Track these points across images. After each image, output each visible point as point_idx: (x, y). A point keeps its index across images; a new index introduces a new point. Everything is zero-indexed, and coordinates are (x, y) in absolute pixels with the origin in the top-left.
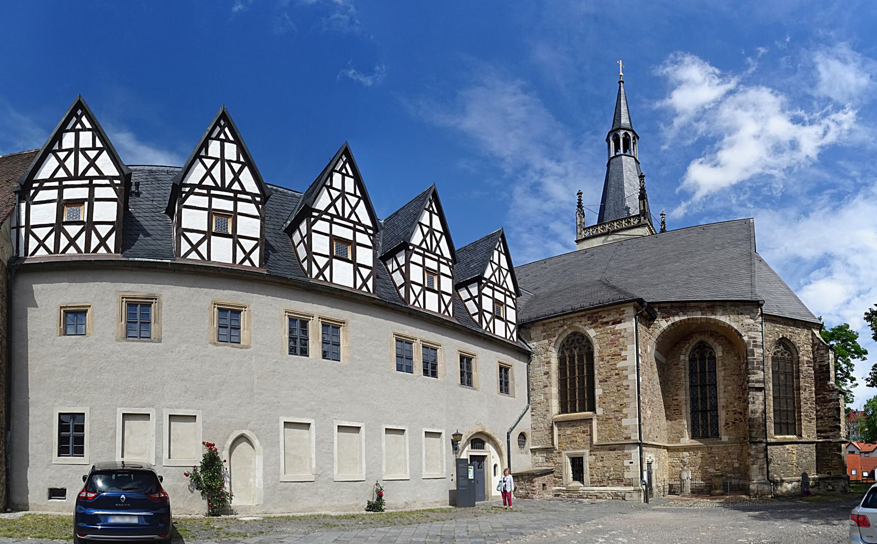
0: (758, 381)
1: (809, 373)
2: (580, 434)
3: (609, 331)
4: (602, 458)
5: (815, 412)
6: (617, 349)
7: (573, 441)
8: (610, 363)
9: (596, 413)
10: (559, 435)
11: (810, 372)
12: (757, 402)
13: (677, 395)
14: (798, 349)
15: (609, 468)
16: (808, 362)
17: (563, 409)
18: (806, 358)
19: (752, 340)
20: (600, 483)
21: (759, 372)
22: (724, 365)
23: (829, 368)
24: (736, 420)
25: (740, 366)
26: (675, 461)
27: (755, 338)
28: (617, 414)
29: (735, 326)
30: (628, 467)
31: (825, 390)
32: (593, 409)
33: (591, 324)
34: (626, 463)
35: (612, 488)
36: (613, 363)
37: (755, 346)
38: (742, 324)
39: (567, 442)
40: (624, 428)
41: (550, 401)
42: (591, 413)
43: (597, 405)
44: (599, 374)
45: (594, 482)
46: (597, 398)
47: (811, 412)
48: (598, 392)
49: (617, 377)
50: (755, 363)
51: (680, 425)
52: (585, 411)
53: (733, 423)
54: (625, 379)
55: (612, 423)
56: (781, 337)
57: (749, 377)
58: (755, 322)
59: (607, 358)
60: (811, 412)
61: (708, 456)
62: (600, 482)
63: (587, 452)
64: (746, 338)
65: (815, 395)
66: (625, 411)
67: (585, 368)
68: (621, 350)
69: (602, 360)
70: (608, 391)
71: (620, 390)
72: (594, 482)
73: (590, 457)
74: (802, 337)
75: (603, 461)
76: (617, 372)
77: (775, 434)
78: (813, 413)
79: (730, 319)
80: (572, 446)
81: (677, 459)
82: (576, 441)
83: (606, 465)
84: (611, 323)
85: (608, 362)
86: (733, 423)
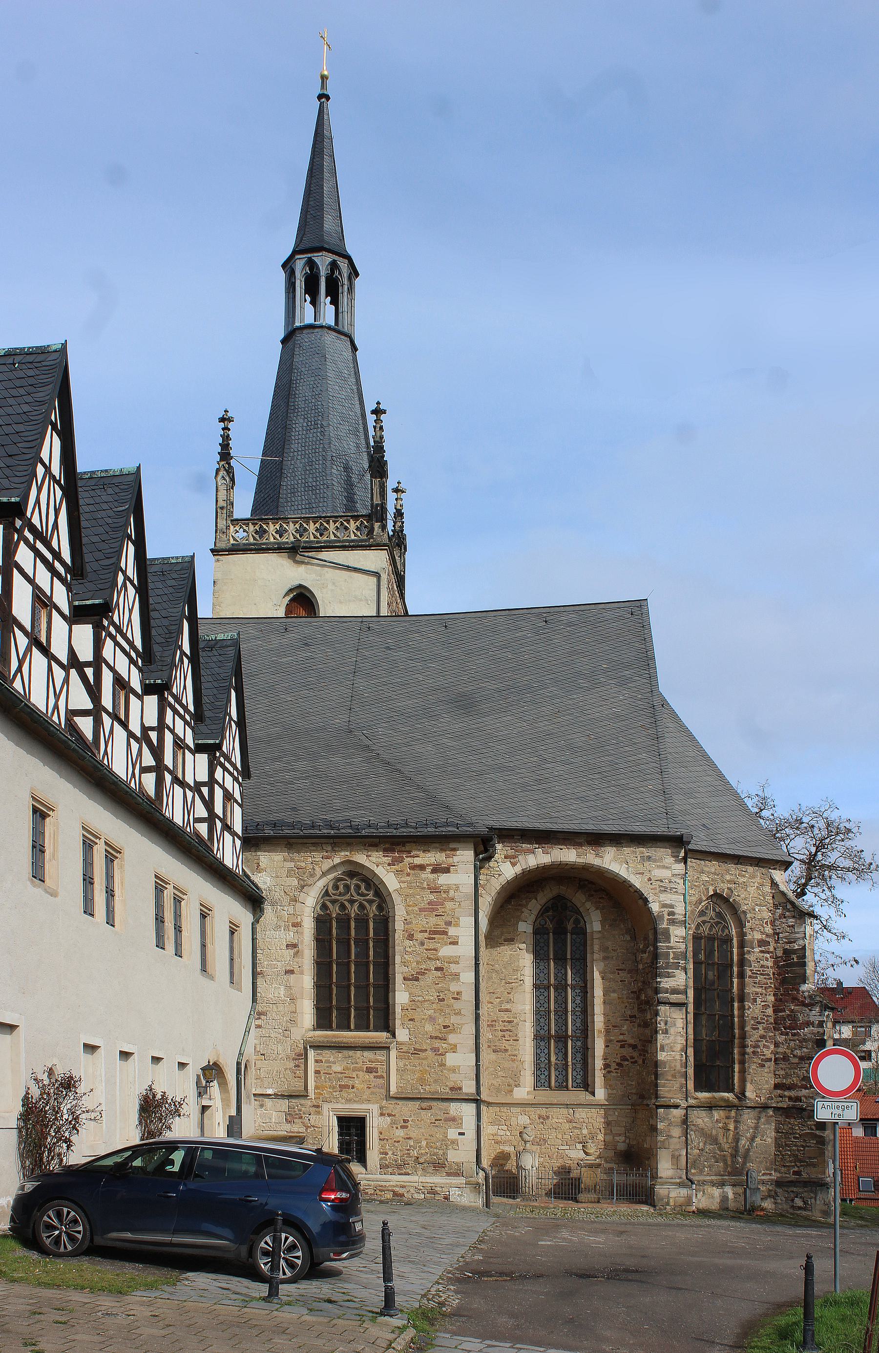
0: (675, 991)
1: (762, 966)
2: (361, 1073)
3: (425, 885)
4: (405, 1121)
5: (772, 1047)
6: (441, 922)
7: (346, 1087)
8: (425, 947)
9: (394, 1036)
10: (317, 1072)
11: (765, 963)
12: (672, 1031)
13: (509, 1001)
14: (742, 916)
15: (418, 1141)
16: (762, 943)
17: (323, 1020)
18: (758, 936)
19: (667, 910)
20: (400, 1168)
21: (677, 972)
22: (604, 949)
23: (804, 956)
24: (624, 1059)
25: (635, 954)
26: (501, 1133)
27: (672, 906)
28: (437, 1044)
29: (637, 882)
30: (454, 1142)
31: (794, 999)
32: (386, 1024)
33: (389, 865)
34: (452, 1134)
35: (422, 1179)
36: (431, 946)
37: (672, 922)
38: (650, 879)
39: (334, 1088)
40: (449, 1070)
41: (298, 1002)
42: (385, 1034)
43: (398, 1022)
44: (404, 963)
45: (387, 1166)
46: (398, 1009)
47: (764, 1046)
48: (401, 997)
49: (439, 974)
50: (672, 956)
51: (513, 1061)
52: (367, 1029)
53: (618, 1064)
54: (453, 980)
55: (426, 1058)
56: (711, 893)
57: (660, 982)
58: (673, 875)
59: (419, 936)
60: (764, 1046)
61: (567, 1126)
62: (399, 1167)
63: (374, 1108)
64: (655, 907)
65: (774, 1011)
66: (452, 1038)
67: (371, 944)
68: (449, 924)
69: (411, 937)
70: (420, 998)
71: (443, 1000)
72: (387, 1166)
73: (381, 1119)
74: (751, 889)
75: (406, 1127)
76: (439, 965)
77: (697, 1089)
78: (768, 1047)
79: (628, 868)
80: (345, 1095)
81: (505, 1128)
82: (353, 1087)
83: (412, 1135)
84: (429, 869)
85: (422, 944)
86: (618, 1064)
